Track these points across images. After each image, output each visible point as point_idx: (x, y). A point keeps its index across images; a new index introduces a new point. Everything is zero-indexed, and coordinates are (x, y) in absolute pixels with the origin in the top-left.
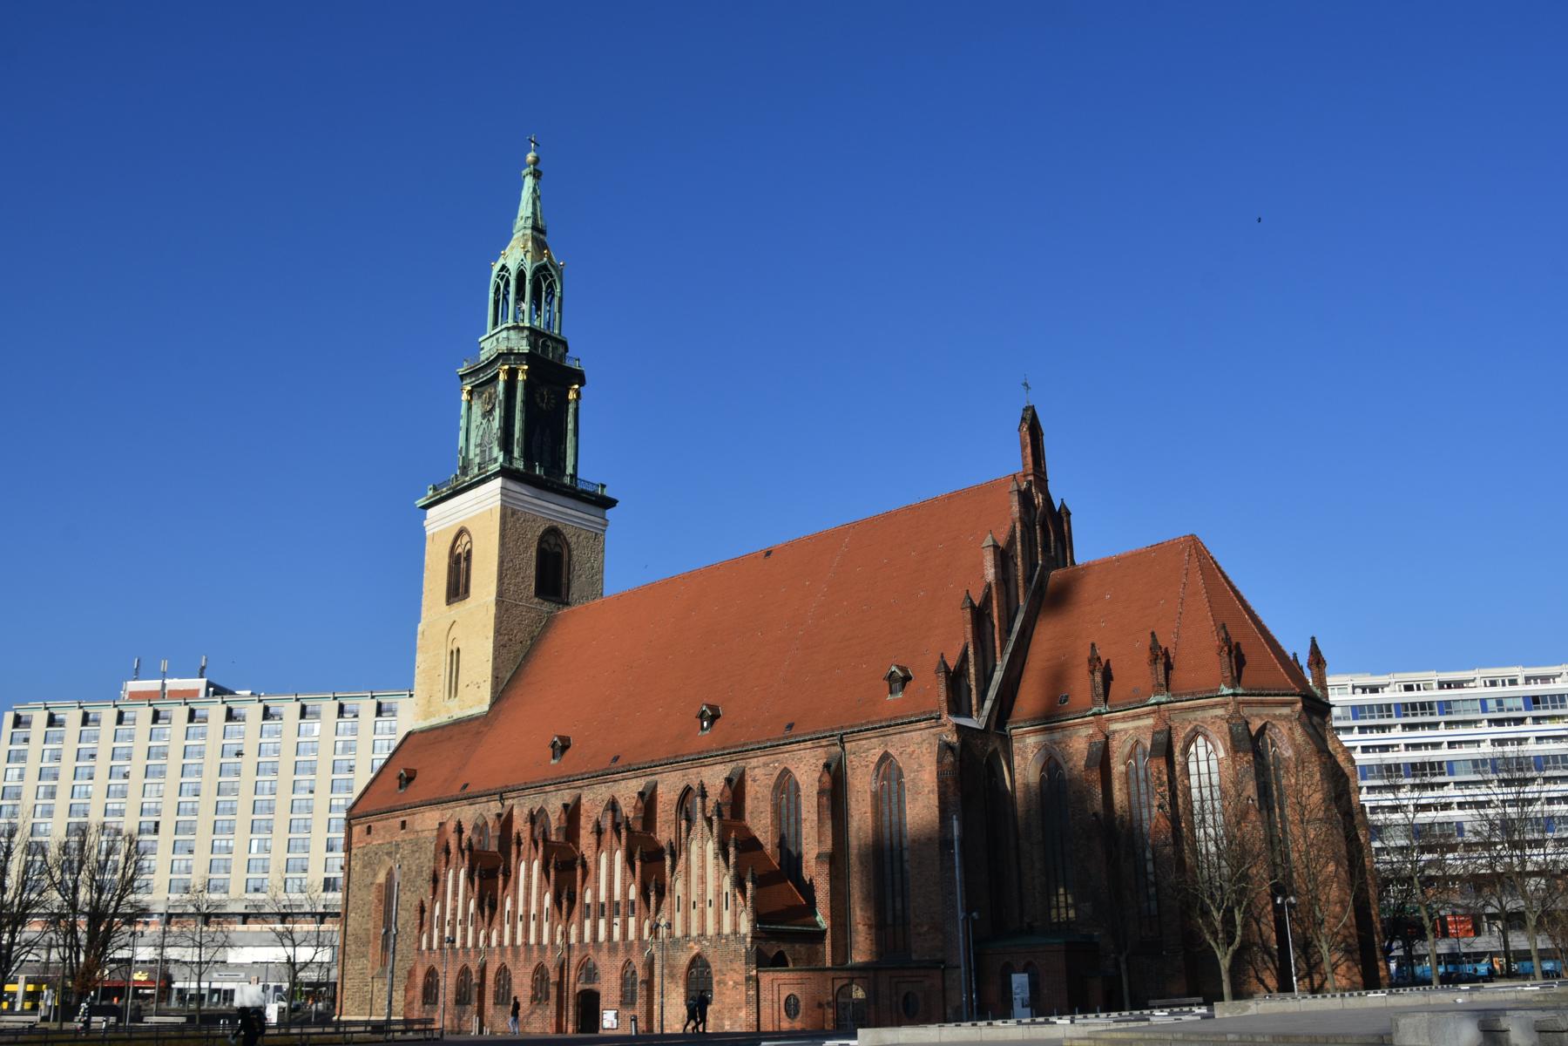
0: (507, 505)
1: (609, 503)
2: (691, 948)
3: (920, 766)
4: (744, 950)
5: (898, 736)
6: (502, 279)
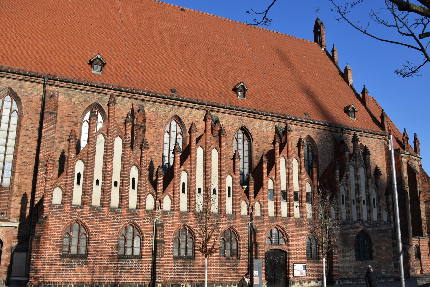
2: (358, 227)
3: (376, 154)
4: (390, 231)
5: (366, 138)
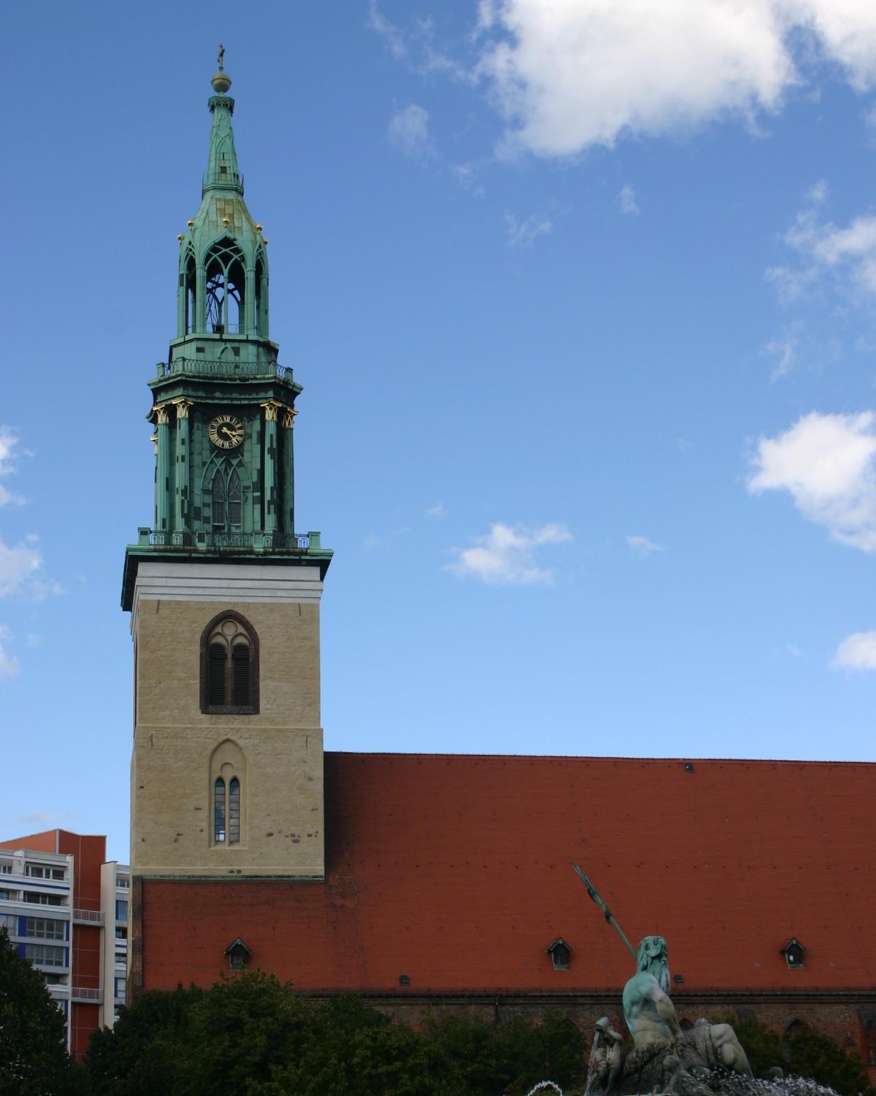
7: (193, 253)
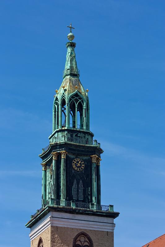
0: (54, 225)
1: (115, 215)
6: (56, 105)
7: (65, 97)
